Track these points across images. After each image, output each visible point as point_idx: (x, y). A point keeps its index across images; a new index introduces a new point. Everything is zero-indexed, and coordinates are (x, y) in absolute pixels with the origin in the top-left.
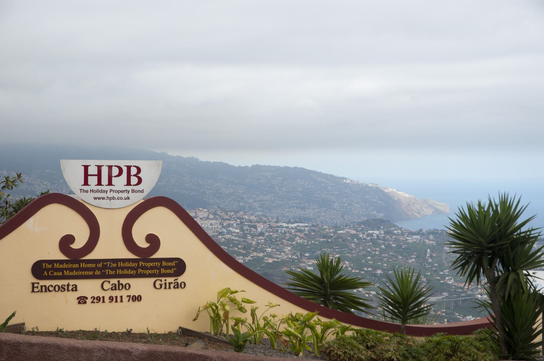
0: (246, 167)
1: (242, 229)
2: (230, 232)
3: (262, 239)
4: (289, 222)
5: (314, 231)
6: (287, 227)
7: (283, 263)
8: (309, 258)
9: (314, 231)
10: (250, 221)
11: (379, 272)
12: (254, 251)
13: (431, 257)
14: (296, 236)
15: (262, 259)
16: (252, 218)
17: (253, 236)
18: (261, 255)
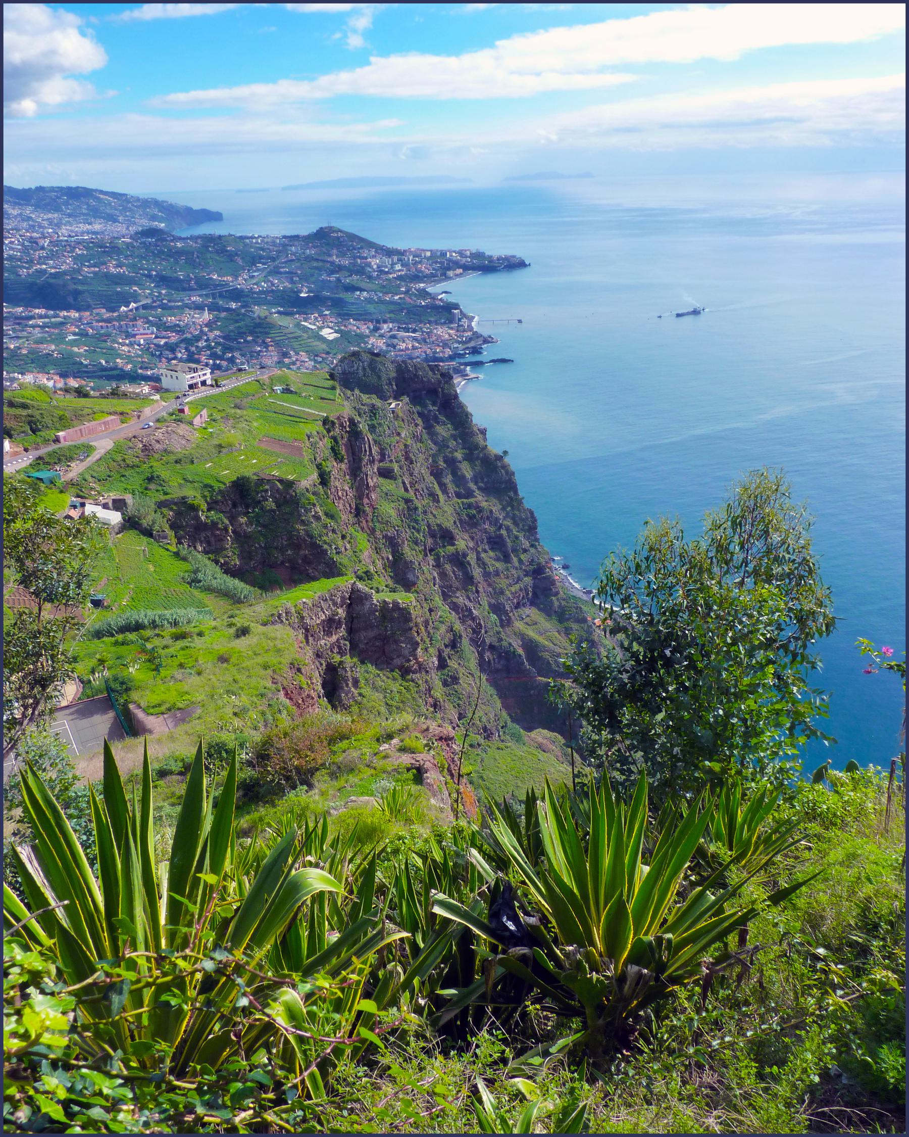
0: (30, 189)
1: (23, 245)
2: (12, 249)
3: (43, 253)
4: (70, 236)
5: (92, 243)
6: (67, 241)
7: (65, 273)
8: (88, 267)
9: (92, 243)
10: (31, 237)
11: (154, 273)
12: (38, 263)
13: (198, 257)
14: (75, 248)
15: (45, 270)
16: (35, 235)
17: (35, 251)
18: (44, 266)
